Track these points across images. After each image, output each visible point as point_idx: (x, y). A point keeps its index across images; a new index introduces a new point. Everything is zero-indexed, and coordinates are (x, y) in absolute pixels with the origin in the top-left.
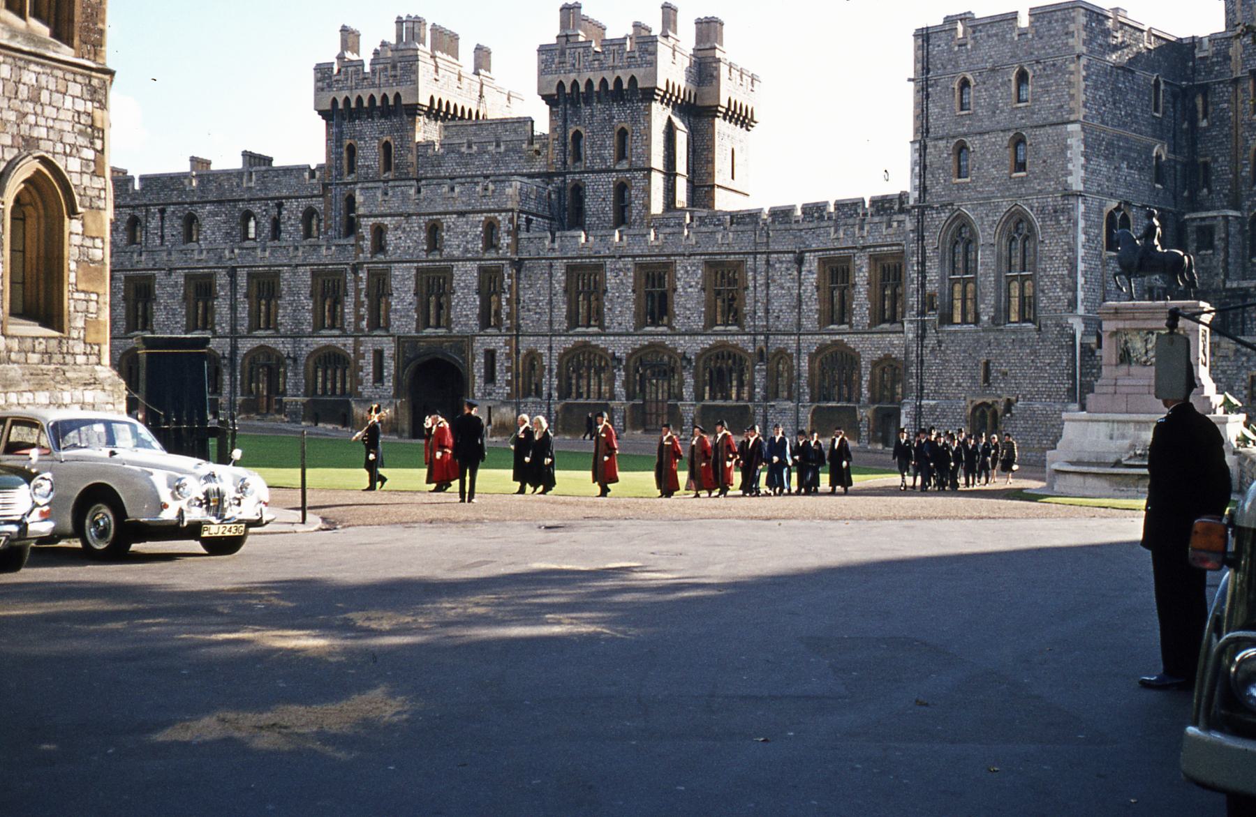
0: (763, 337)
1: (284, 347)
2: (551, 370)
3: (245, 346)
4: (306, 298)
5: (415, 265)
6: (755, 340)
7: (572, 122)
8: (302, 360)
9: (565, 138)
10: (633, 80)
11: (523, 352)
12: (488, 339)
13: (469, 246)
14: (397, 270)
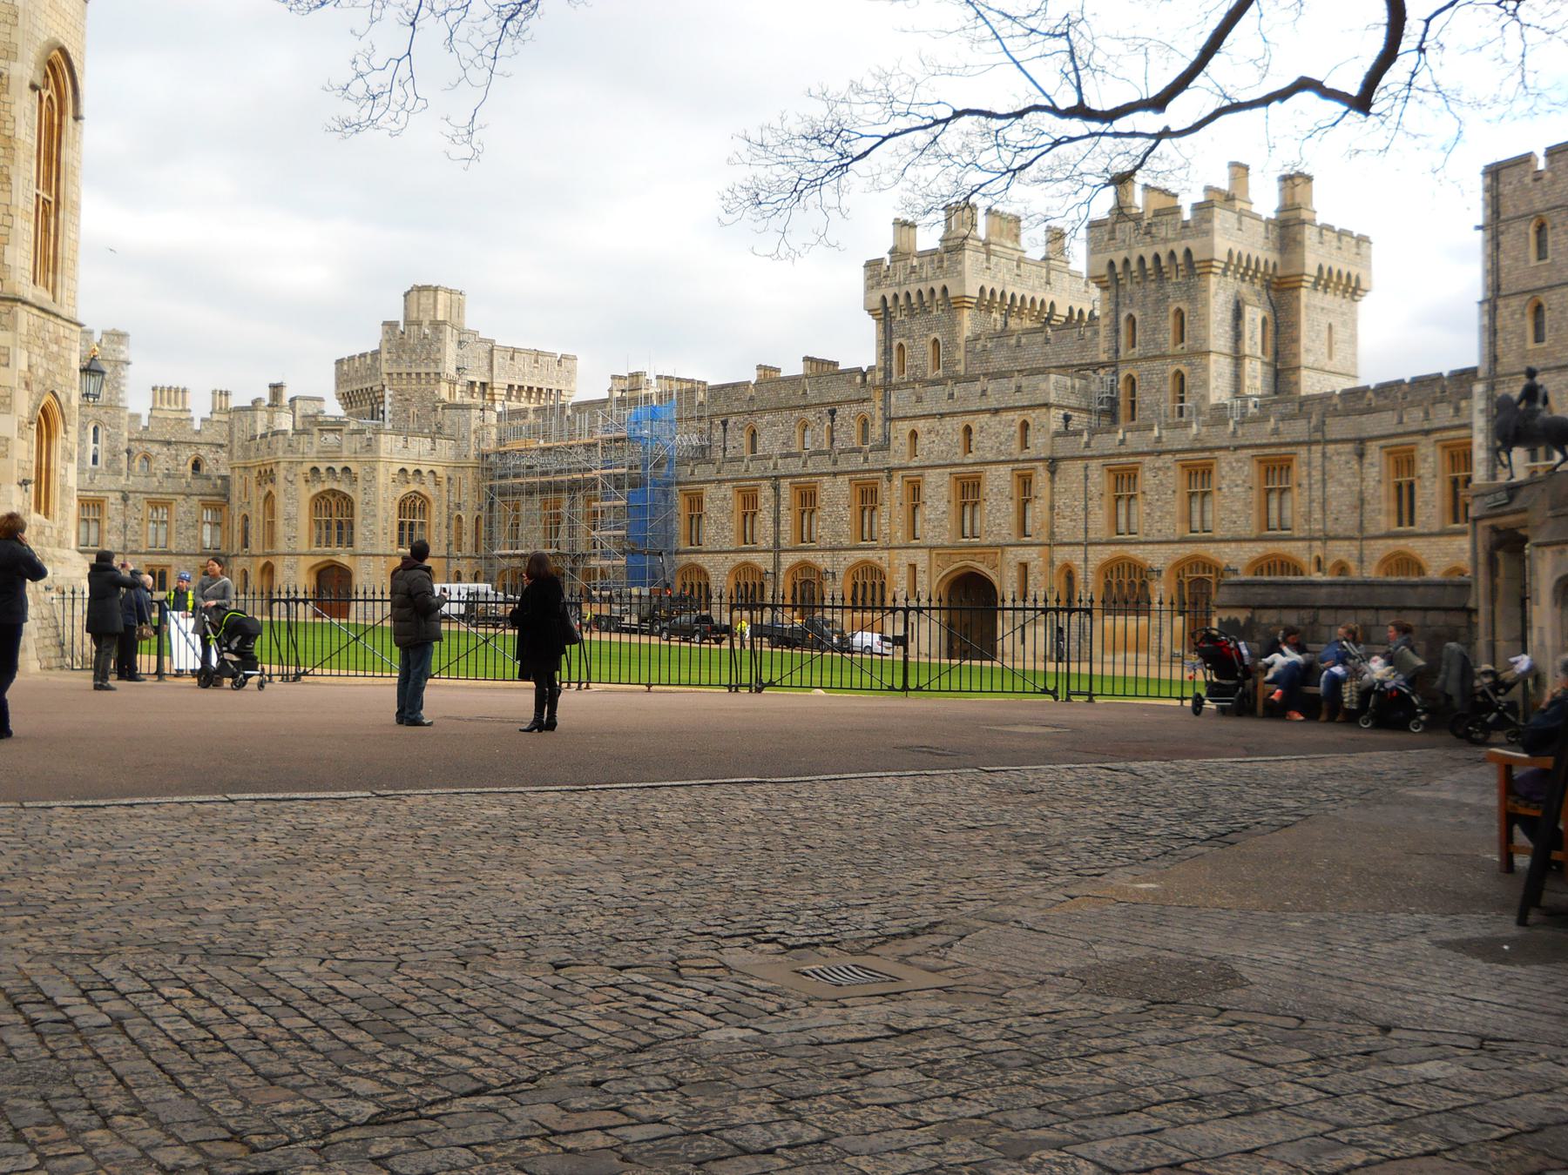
0: (1319, 543)
1: (823, 561)
2: (1086, 582)
3: (788, 560)
6: (1310, 547)
8: (840, 575)
9: (1117, 321)
10: (1188, 252)
11: (1058, 563)
12: (1021, 550)
13: (1002, 448)
14: (932, 477)
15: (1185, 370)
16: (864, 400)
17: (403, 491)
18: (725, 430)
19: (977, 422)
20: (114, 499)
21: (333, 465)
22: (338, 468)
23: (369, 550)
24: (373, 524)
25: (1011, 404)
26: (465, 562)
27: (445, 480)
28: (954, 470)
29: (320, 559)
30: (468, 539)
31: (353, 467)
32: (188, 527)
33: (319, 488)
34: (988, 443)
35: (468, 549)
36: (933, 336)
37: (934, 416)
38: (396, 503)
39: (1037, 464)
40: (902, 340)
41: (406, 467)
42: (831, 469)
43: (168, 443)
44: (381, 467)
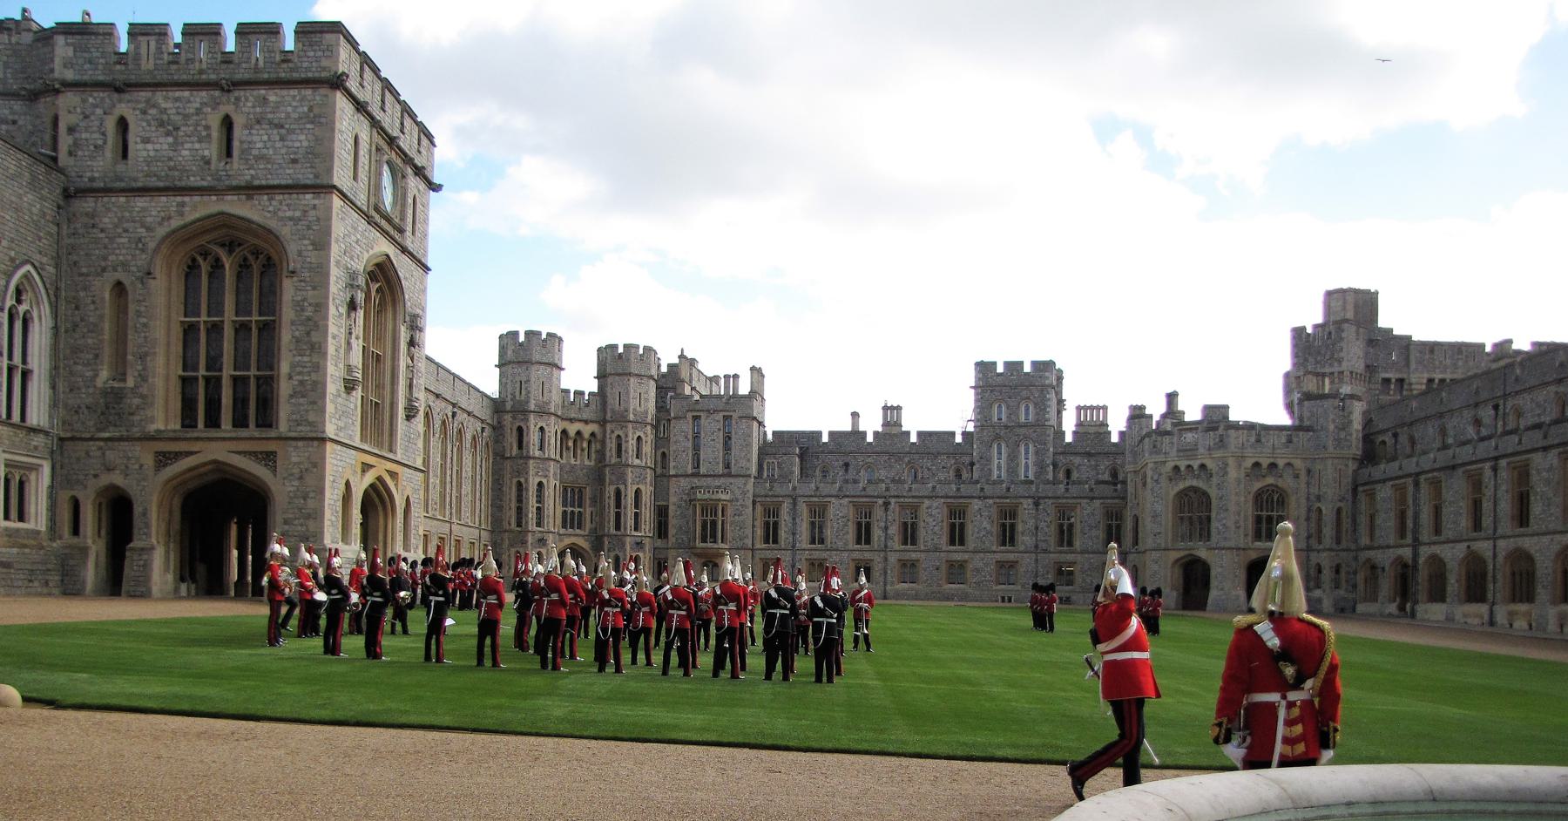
17: (1258, 485)
20: (1027, 504)
21: (1191, 463)
22: (1196, 464)
23: (1223, 544)
24: (1225, 518)
26: (1325, 554)
27: (1303, 474)
29: (1182, 554)
30: (1328, 531)
31: (1210, 464)
32: (1091, 527)
33: (1181, 486)
35: (1328, 540)
38: (1251, 497)
41: (1261, 460)
43: (1089, 455)
44: (1231, 461)
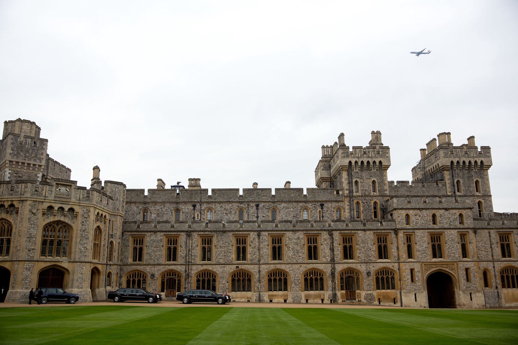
3: (339, 268)
4: (371, 245)
5: (427, 231)
7: (456, 177)
9: (453, 182)
14: (418, 233)
15: (483, 201)
16: (340, 201)
18: (257, 209)
19: (438, 213)
21: (63, 206)
23: (83, 259)
24: (87, 243)
25: (454, 207)
28: (429, 231)
31: (77, 209)
34: (445, 221)
36: (373, 179)
37: (419, 209)
39: (469, 230)
40: (357, 179)
42: (362, 227)
44: (92, 209)
